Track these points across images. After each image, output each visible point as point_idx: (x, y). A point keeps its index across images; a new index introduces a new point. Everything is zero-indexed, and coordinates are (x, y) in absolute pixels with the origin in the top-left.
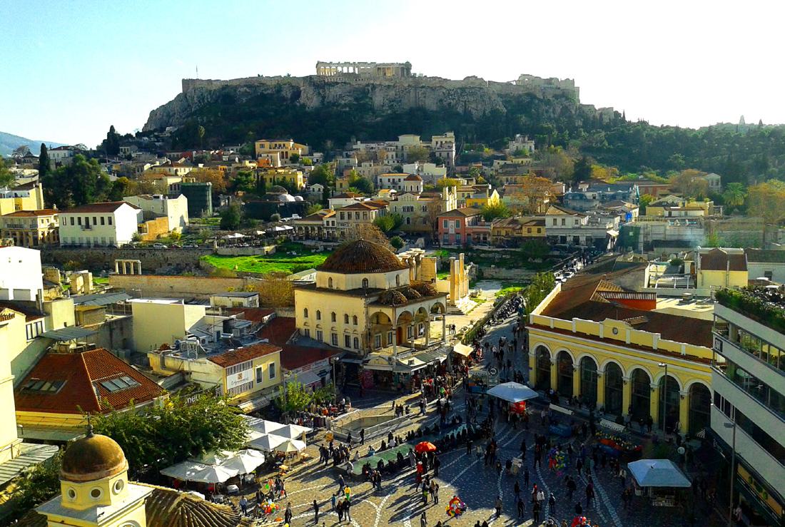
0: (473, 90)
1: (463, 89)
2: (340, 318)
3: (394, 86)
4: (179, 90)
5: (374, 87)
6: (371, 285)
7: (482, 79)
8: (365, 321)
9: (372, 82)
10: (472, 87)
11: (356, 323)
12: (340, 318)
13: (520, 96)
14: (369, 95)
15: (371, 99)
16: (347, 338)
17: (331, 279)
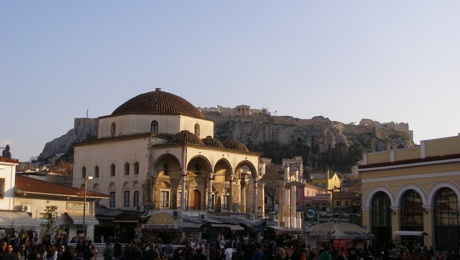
0: (320, 128)
1: (311, 127)
2: (120, 169)
3: (251, 123)
4: (72, 126)
5: (234, 123)
6: (162, 130)
7: (327, 119)
8: (148, 167)
9: (232, 119)
10: (320, 125)
11: (137, 171)
12: (120, 169)
13: (361, 135)
14: (229, 130)
15: (231, 133)
16: (127, 193)
17: (114, 125)
